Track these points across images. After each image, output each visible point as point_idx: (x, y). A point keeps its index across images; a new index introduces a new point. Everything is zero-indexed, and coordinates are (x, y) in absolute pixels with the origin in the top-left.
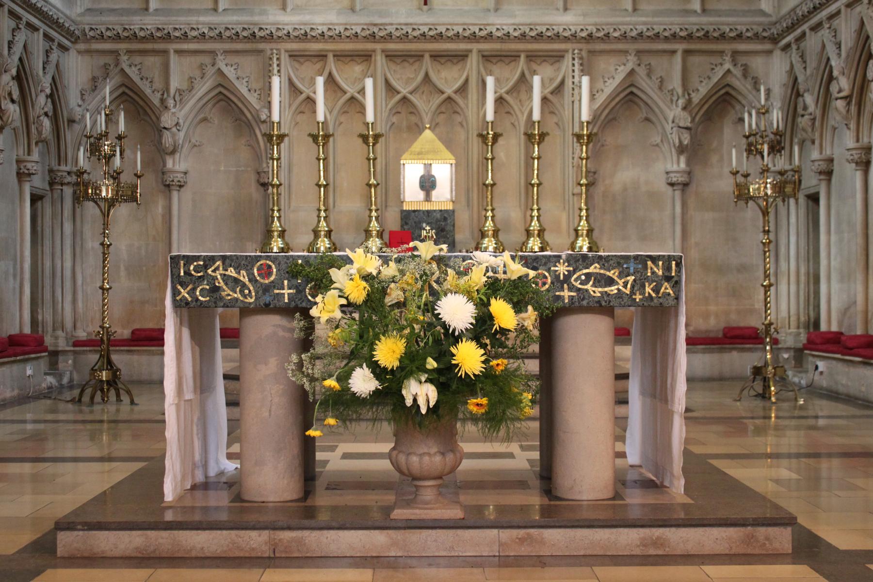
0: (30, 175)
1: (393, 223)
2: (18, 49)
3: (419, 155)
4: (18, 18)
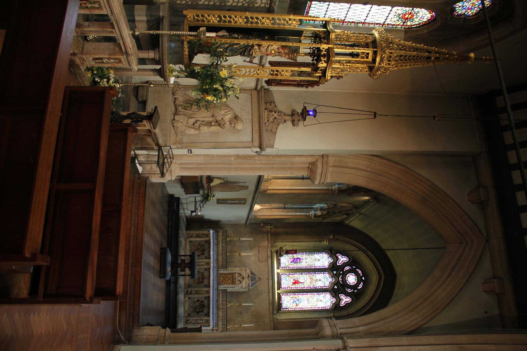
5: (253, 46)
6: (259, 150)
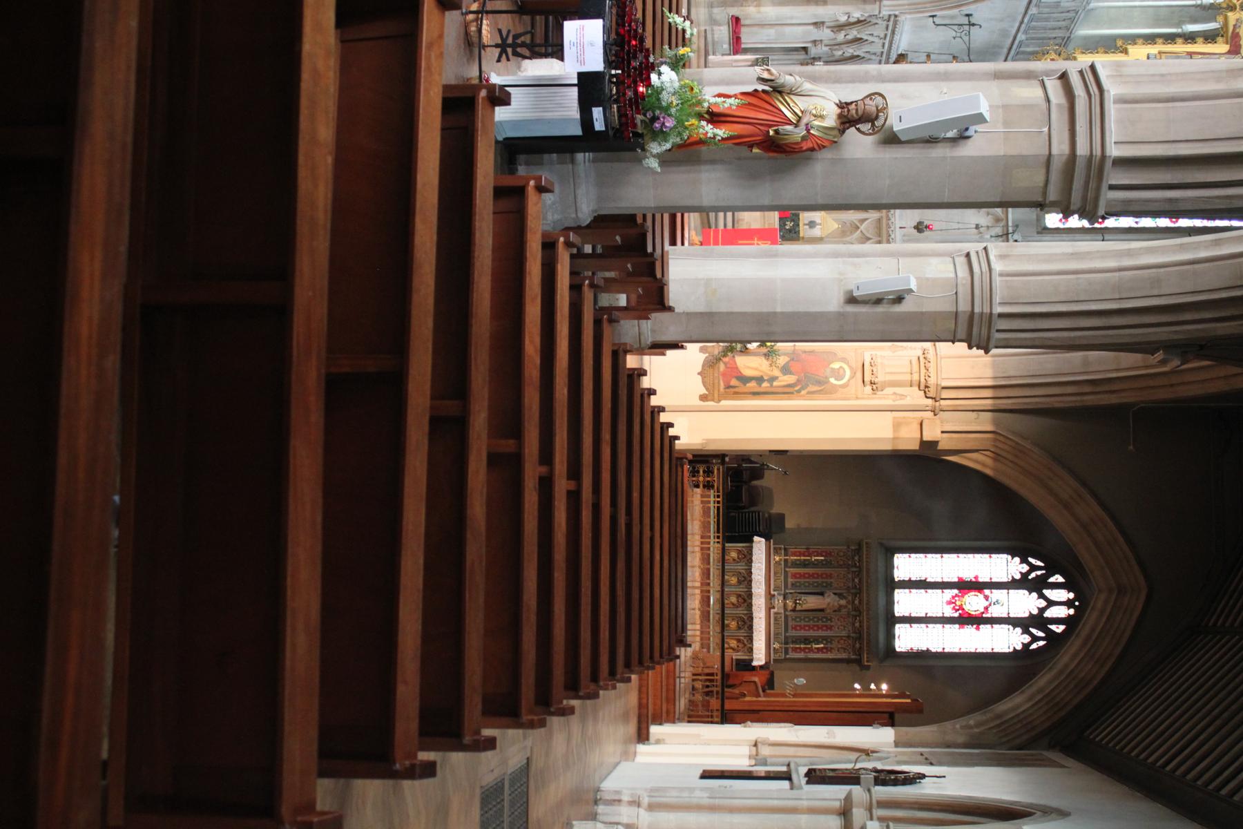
0: (815, 46)
2: (871, 39)
4: (885, 38)
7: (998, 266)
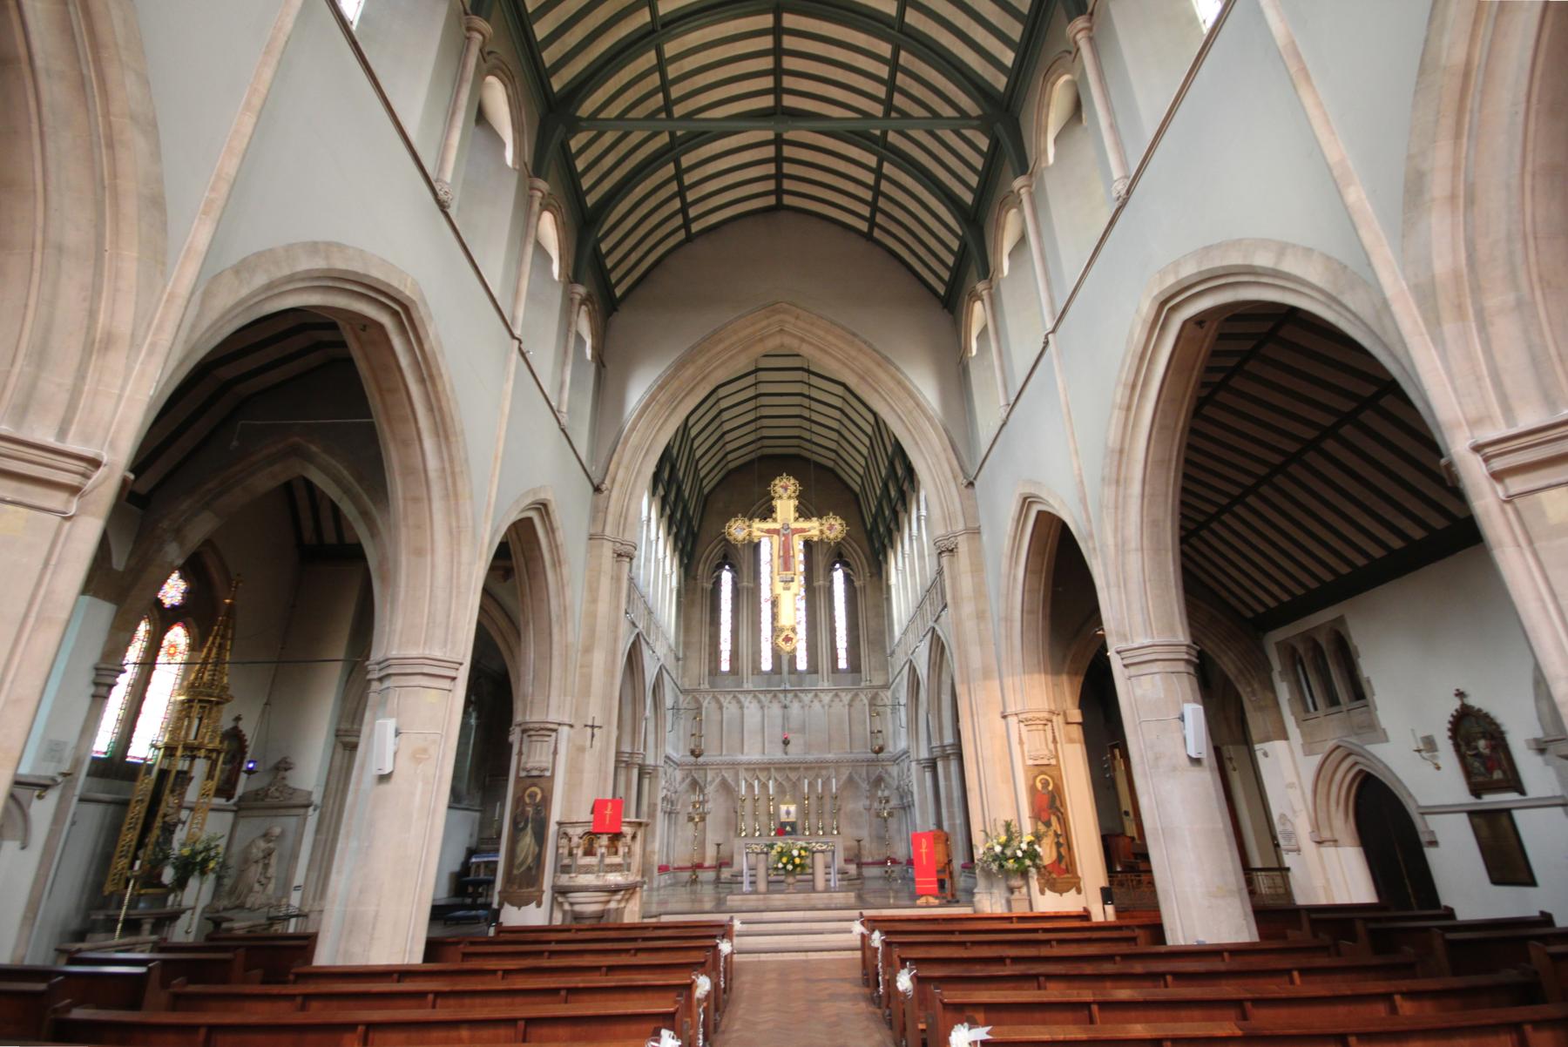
1: (778, 826)
3: (785, 804)
5: (164, 822)
6: (311, 809)
7: (1147, 641)
